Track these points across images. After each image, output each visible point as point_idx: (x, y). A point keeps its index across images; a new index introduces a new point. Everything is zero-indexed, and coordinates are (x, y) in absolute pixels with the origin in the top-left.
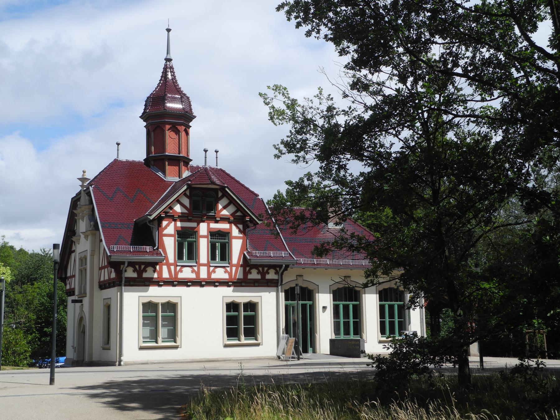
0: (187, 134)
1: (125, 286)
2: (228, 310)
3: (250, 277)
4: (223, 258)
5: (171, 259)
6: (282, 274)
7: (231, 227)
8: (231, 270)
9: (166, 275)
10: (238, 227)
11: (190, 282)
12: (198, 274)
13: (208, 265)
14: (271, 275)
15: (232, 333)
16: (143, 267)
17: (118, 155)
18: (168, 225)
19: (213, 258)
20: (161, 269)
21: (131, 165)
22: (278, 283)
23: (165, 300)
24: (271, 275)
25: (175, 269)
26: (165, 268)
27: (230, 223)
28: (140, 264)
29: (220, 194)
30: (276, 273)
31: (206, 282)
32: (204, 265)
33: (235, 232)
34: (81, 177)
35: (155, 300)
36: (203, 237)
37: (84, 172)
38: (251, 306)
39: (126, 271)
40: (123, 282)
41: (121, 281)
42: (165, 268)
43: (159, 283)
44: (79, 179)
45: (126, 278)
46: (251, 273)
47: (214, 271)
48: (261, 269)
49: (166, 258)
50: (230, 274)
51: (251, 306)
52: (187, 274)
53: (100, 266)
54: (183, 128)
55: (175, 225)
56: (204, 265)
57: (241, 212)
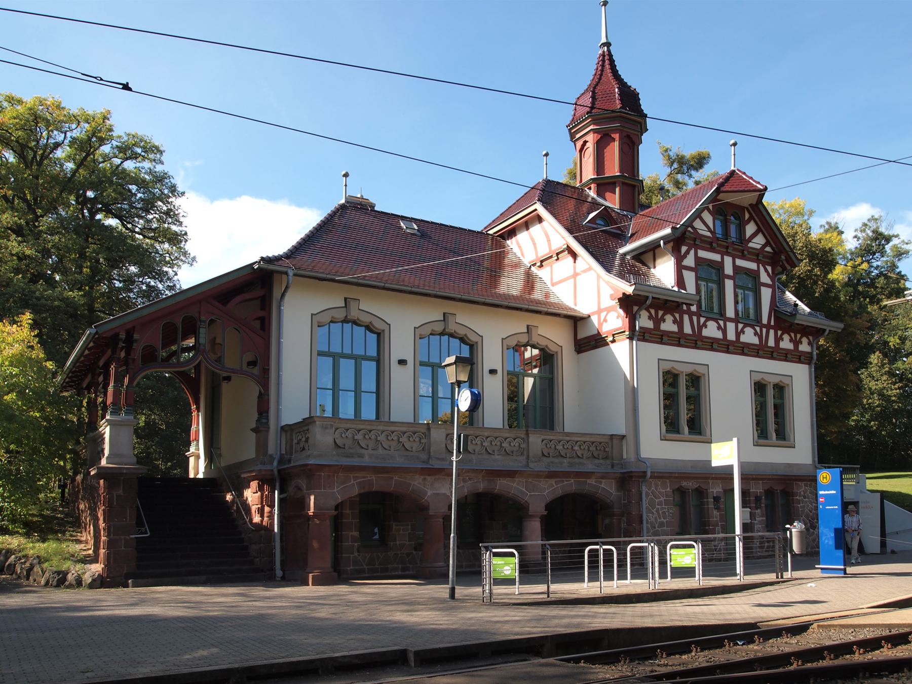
7: (758, 267)
8: (761, 331)
9: (687, 330)
10: (766, 271)
12: (724, 332)
18: (687, 252)
26: (686, 317)
27: (758, 261)
29: (747, 216)
32: (730, 320)
42: (686, 317)
43: (678, 340)
50: (760, 337)
52: (711, 330)
56: (730, 320)
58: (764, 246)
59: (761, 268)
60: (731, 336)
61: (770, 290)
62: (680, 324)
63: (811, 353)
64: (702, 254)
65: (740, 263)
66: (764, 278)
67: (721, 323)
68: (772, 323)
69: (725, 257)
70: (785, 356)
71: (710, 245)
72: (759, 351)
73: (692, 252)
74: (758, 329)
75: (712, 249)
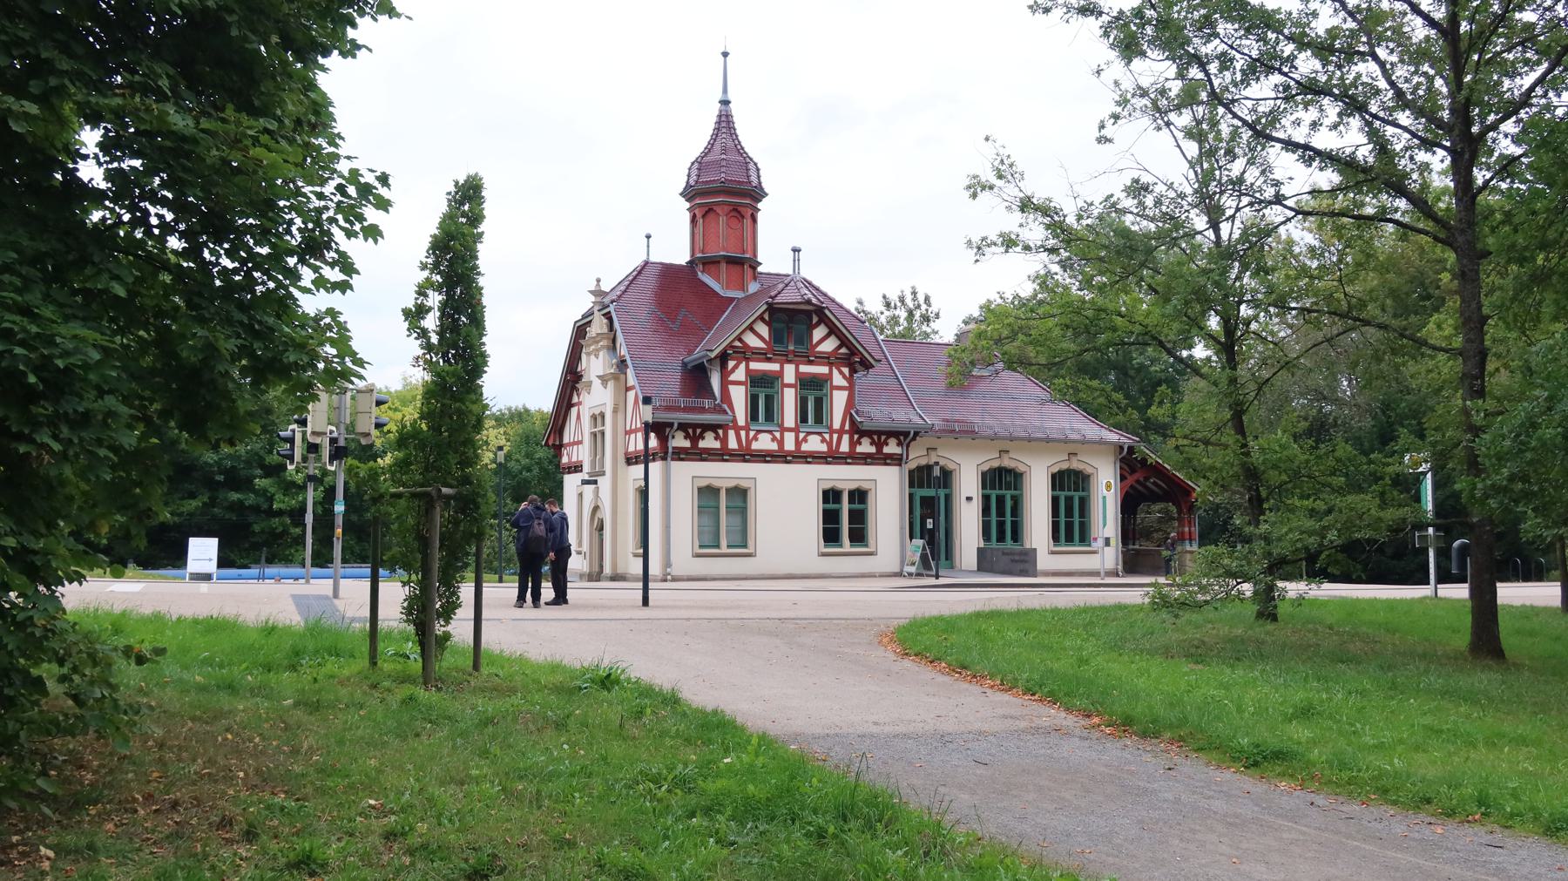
0: (754, 220)
1: (673, 459)
2: (826, 500)
3: (859, 449)
4: (819, 420)
5: (741, 422)
6: (908, 446)
9: (733, 444)
10: (841, 373)
11: (768, 456)
12: (781, 443)
13: (796, 430)
14: (892, 448)
15: (831, 536)
16: (699, 431)
17: (648, 255)
18: (736, 367)
19: (804, 420)
20: (726, 435)
21: (669, 273)
22: (901, 459)
23: (731, 484)
24: (892, 448)
25: (747, 435)
27: (830, 365)
28: (695, 426)
29: (815, 319)
30: (898, 445)
31: (794, 457)
32: (790, 430)
33: (838, 380)
34: (593, 289)
35: (716, 483)
36: (789, 386)
37: (598, 281)
38: (859, 496)
39: (673, 437)
40: (670, 454)
41: (666, 453)
42: (731, 433)
43: (723, 455)
44: (591, 292)
45: (674, 448)
46: (860, 444)
47: (805, 440)
48: (875, 437)
49: (735, 420)
50: (830, 444)
51: (859, 496)
52: (764, 443)
53: (628, 428)
54: (750, 212)
55: (747, 366)
56: (790, 430)
57: (848, 348)
58: (839, 347)
59: (835, 371)
60: (790, 445)
61: (845, 394)
62: (724, 441)
63: (902, 455)
64: (754, 366)
65: (804, 369)
66: (838, 380)
67: (778, 435)
68: (847, 427)
69: (786, 366)
70: (866, 459)
71: (763, 356)
72: (831, 457)
73: (743, 366)
74: (827, 436)
75: (769, 360)
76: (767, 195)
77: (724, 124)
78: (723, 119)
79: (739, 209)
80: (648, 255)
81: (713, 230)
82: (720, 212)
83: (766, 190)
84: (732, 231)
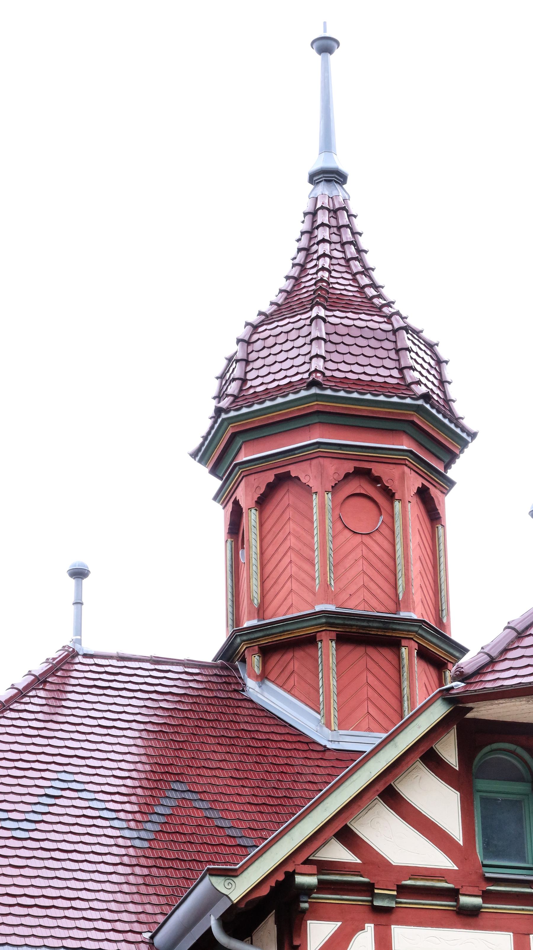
17: (78, 630)
76: (473, 435)
77: (322, 233)
78: (323, 217)
79: (378, 470)
80: (78, 630)
81: (292, 541)
82: (314, 484)
83: (468, 423)
84: (358, 538)
